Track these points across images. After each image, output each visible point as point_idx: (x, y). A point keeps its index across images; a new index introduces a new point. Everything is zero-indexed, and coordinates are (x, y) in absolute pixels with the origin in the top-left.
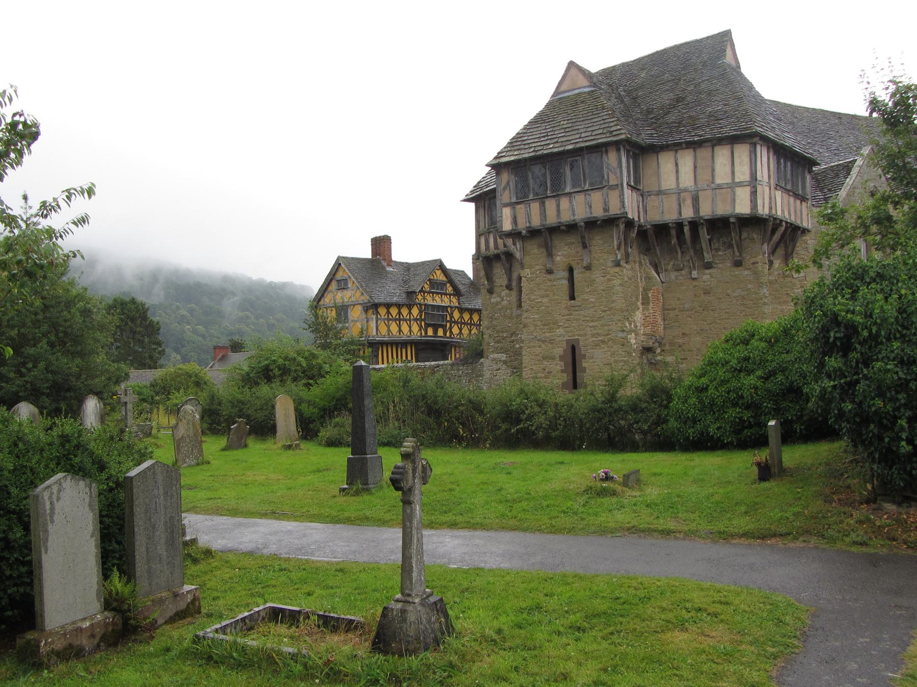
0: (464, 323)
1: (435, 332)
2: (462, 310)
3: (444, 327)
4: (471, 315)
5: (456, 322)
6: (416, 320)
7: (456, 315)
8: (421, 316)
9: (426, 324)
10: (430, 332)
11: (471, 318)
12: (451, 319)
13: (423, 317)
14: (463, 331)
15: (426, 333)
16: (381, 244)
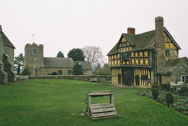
0: (137, 58)
1: (126, 63)
2: (134, 53)
3: (129, 60)
4: (139, 53)
5: (133, 58)
6: (119, 59)
7: (133, 54)
8: (120, 58)
9: (122, 60)
10: (124, 63)
11: (139, 55)
12: (131, 57)
13: (121, 58)
14: (140, 62)
15: (122, 63)
16: (131, 30)
